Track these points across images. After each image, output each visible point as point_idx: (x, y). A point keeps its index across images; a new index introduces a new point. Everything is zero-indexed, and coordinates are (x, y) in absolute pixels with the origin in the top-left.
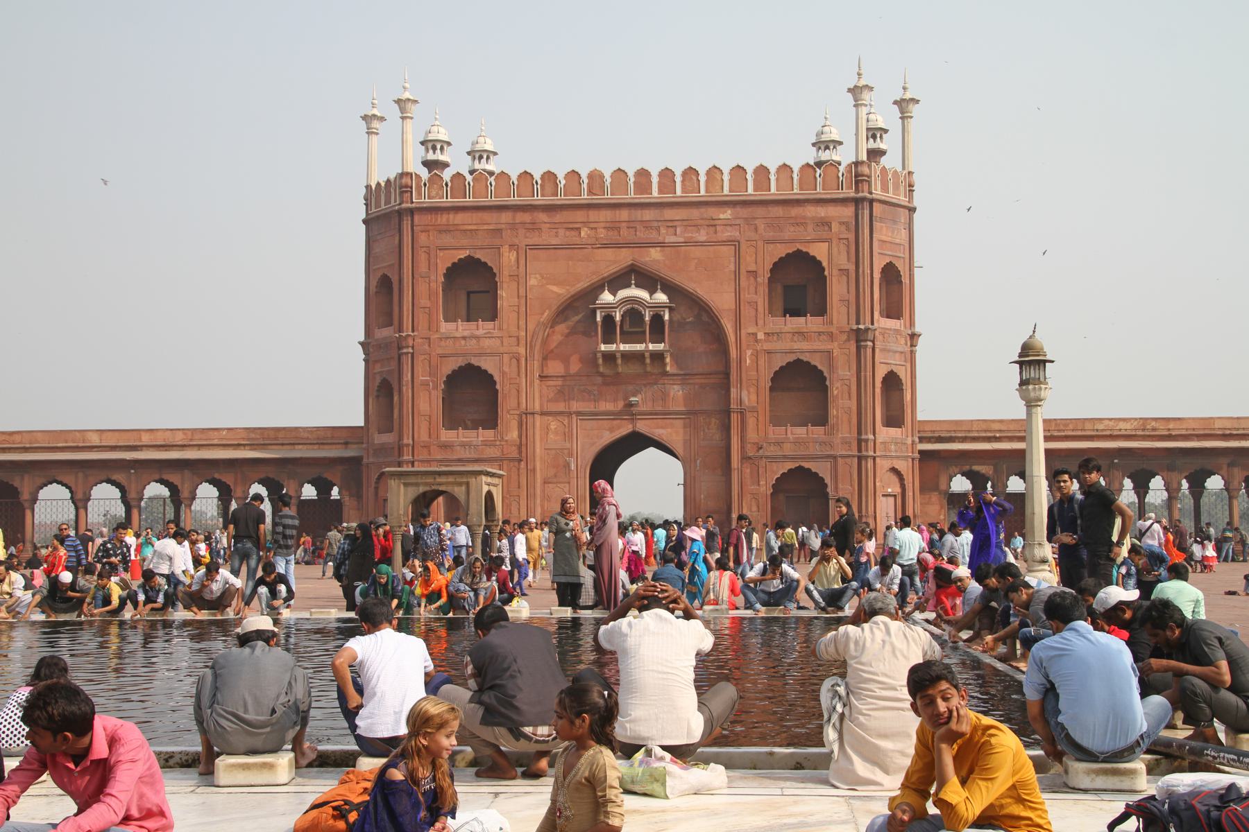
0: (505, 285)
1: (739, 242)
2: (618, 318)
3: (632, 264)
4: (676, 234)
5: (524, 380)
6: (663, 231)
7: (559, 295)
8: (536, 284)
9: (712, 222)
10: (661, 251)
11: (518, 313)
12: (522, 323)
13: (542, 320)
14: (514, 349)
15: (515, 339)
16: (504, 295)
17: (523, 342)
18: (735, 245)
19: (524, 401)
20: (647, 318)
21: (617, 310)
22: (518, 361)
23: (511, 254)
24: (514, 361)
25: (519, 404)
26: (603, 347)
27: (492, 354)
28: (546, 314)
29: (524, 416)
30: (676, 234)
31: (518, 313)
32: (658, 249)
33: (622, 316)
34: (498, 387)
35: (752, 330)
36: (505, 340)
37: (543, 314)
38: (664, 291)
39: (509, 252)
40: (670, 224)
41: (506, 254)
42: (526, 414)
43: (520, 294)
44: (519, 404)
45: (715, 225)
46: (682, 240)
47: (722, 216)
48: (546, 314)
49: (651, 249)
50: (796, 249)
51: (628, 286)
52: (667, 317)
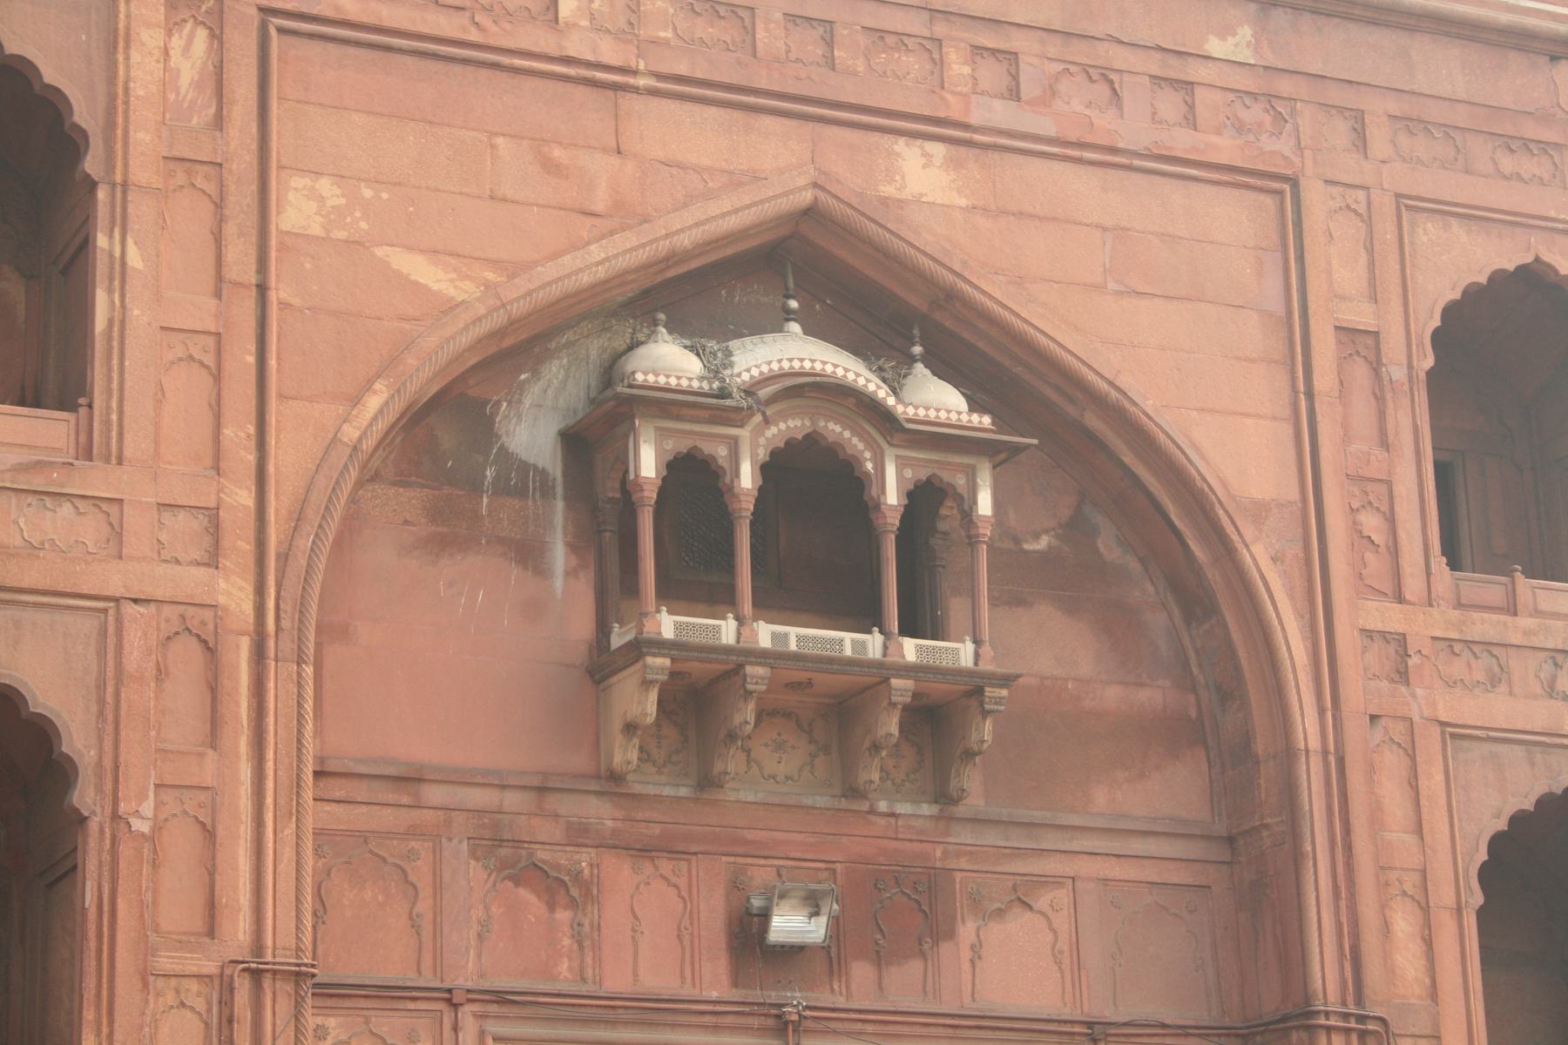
0: (141, 210)
1: (1294, 182)
2: (747, 478)
3: (810, 213)
4: (1014, 94)
5: (245, 772)
6: (958, 67)
7: (451, 308)
8: (316, 230)
9: (1176, 68)
10: (953, 164)
11: (217, 376)
12: (239, 432)
13: (350, 433)
14: (191, 581)
15: (197, 523)
16: (134, 258)
17: (240, 544)
18: (1280, 193)
19: (244, 897)
20: (892, 496)
21: (744, 433)
22: (210, 650)
23: (177, 42)
24: (186, 656)
25: (211, 906)
26: (667, 625)
27: (56, 598)
28: (373, 403)
29: (243, 987)
30: (1014, 94)
31: (217, 376)
32: (938, 150)
33: (768, 470)
34: (85, 796)
35: (1384, 616)
36: (134, 521)
37: (356, 400)
38: (946, 369)
39: (169, 34)
40: (988, 40)
41: (149, 38)
42: (256, 975)
43: (232, 272)
44: (211, 906)
45: (1188, 86)
46: (1045, 125)
47: (1216, 47)
48: (373, 403)
49: (901, 145)
50: (1529, 259)
51: (768, 324)
52: (985, 504)
